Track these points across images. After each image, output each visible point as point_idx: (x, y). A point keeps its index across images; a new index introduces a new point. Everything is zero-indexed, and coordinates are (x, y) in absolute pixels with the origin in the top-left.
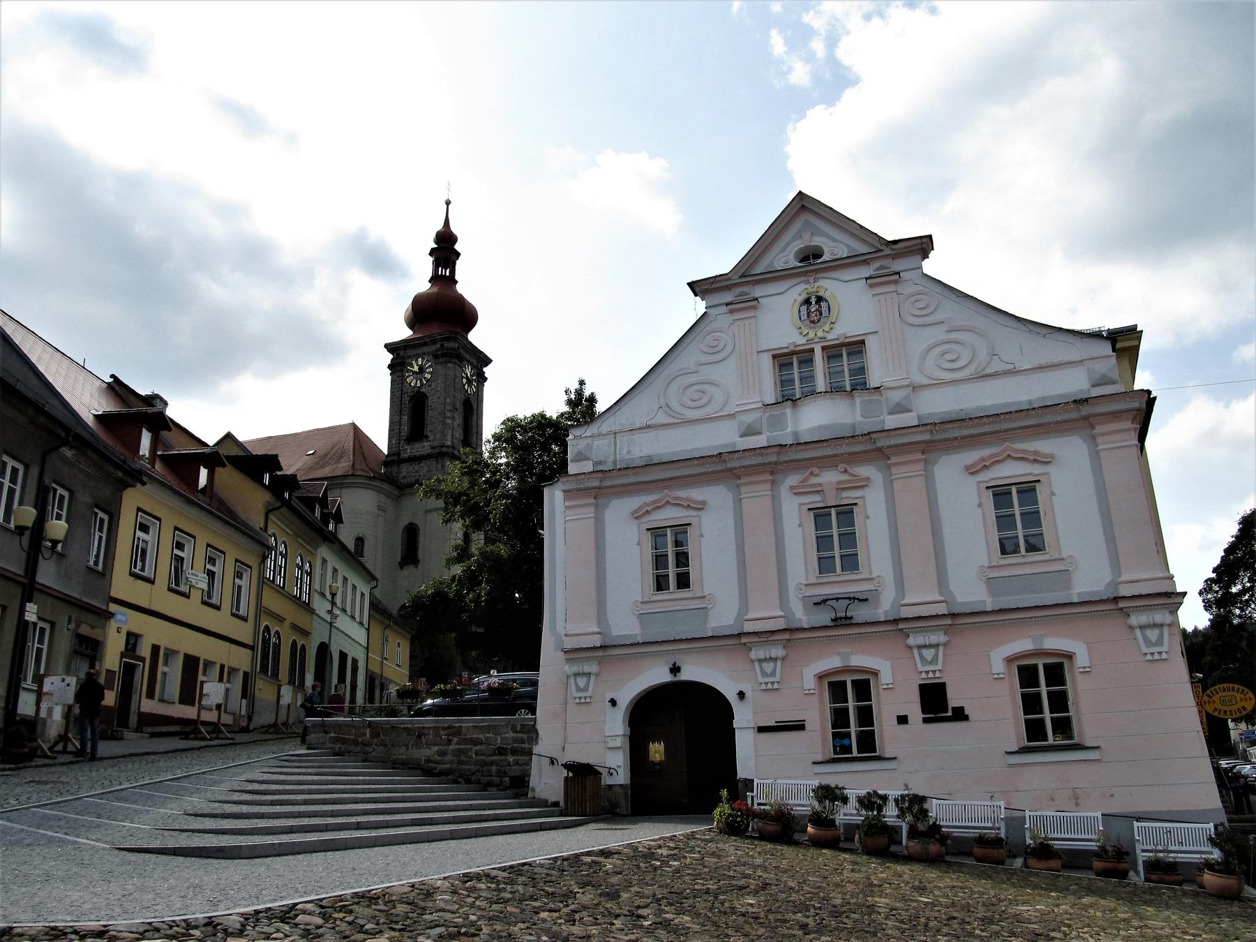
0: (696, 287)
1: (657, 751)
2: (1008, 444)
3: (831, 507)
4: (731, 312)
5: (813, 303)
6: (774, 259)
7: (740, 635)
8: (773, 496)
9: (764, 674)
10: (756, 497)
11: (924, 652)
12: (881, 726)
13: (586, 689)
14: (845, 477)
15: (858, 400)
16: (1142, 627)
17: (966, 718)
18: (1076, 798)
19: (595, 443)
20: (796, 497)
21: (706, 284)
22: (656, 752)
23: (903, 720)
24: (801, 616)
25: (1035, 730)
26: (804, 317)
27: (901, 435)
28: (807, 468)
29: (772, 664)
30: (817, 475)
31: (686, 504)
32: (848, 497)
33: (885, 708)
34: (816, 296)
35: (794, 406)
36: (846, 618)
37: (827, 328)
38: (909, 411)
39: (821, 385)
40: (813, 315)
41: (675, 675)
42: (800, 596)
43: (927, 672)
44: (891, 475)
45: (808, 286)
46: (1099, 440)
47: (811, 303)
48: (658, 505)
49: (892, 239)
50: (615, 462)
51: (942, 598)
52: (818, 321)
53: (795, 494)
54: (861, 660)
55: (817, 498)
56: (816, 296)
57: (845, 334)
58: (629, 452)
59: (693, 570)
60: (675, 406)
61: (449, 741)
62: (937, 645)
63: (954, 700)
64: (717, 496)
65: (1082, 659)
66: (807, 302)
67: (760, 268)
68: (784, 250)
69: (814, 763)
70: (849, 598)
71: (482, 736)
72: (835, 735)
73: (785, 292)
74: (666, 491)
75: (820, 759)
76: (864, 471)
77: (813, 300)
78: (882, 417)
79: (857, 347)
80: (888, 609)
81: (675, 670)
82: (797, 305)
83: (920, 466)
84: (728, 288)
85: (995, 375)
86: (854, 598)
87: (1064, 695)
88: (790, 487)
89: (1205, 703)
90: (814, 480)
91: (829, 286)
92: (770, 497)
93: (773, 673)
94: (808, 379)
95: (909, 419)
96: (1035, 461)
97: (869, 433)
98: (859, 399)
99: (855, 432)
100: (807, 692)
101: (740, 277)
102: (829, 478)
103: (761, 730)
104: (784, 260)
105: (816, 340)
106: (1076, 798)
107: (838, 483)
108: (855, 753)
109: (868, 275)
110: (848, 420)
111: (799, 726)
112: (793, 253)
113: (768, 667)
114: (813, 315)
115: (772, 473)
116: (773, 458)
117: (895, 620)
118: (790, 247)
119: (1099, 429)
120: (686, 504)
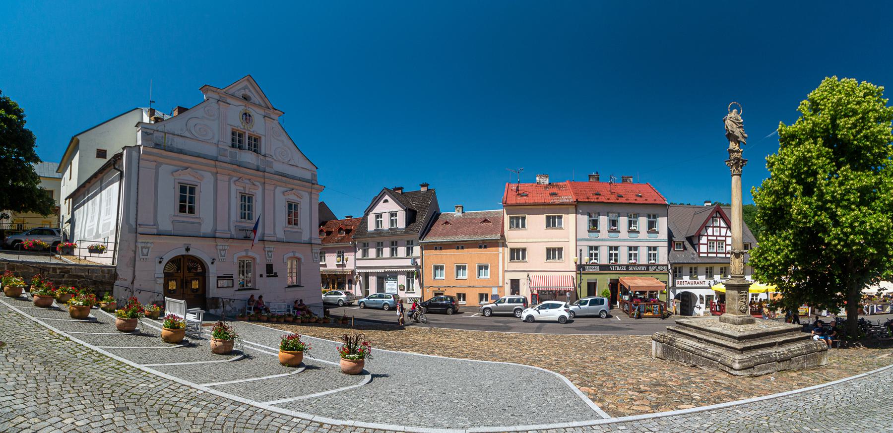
17: (277, 276)
23: (261, 276)
58: (171, 144)
61: (63, 276)
66: (245, 114)
71: (83, 274)
81: (188, 250)
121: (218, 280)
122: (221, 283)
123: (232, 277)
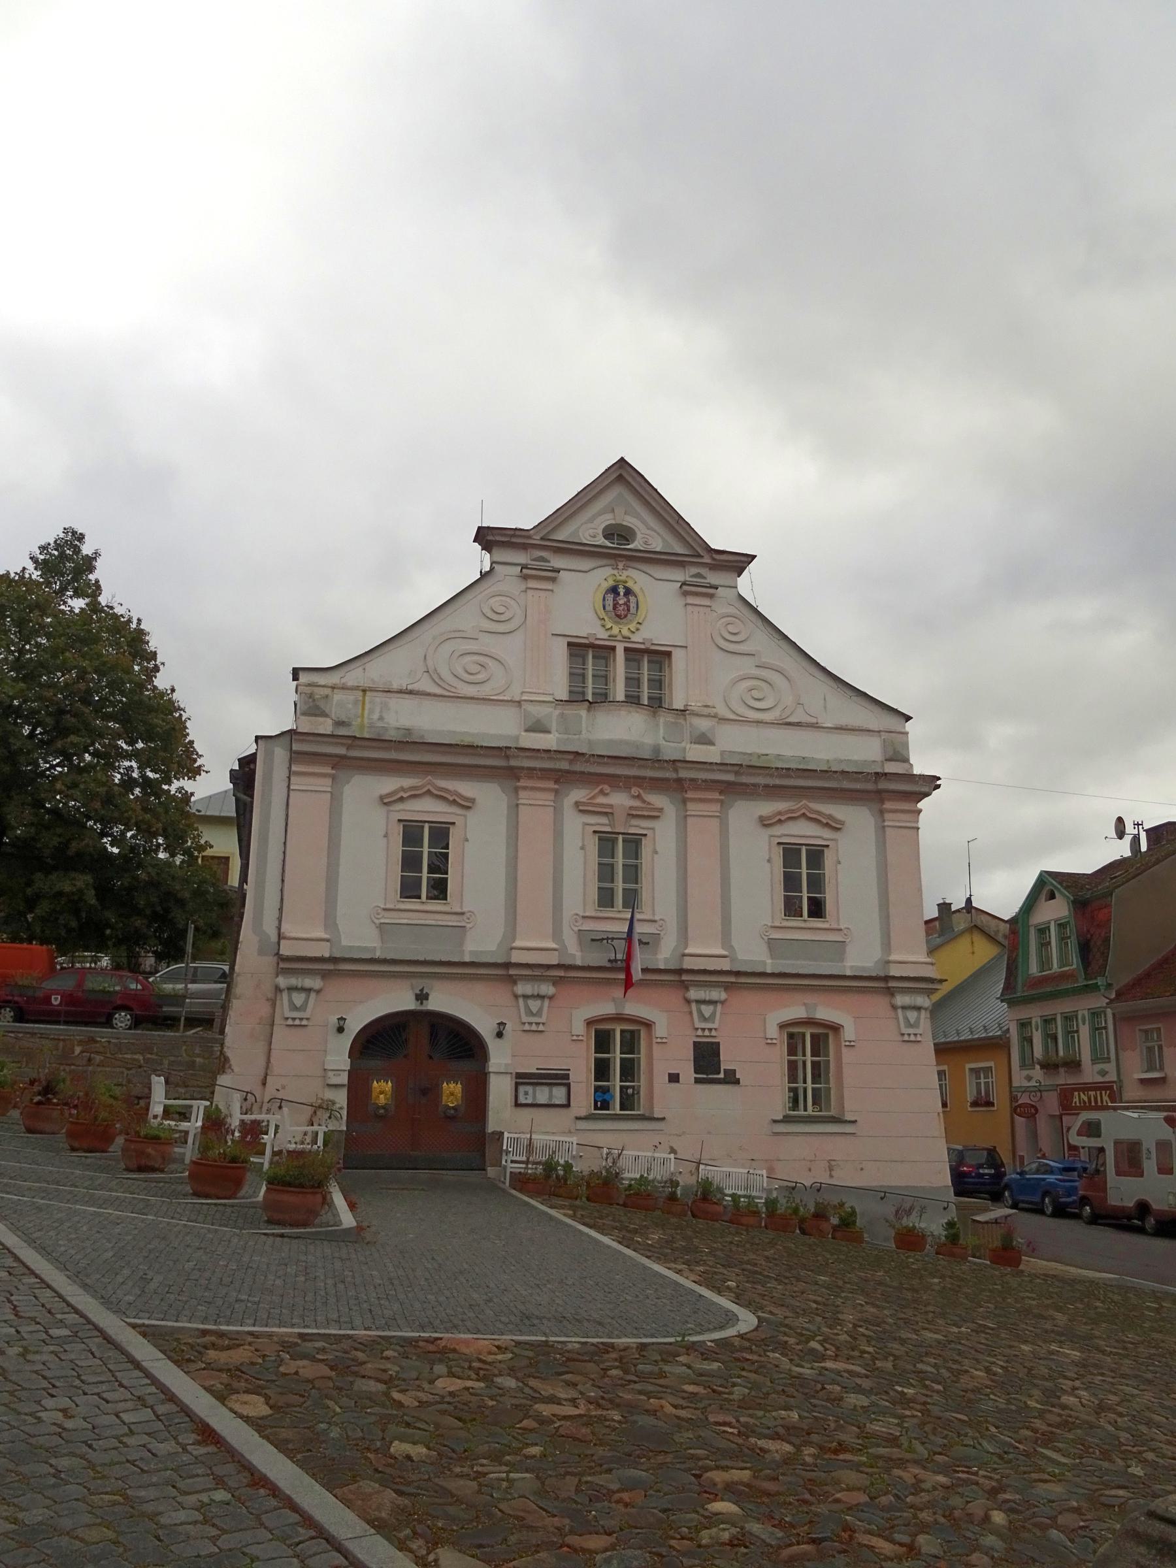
0: (486, 538)
1: (382, 1090)
3: (619, 833)
5: (622, 594)
6: (579, 528)
9: (530, 1013)
13: (303, 1008)
20: (581, 814)
22: (381, 1093)
24: (576, 954)
26: (610, 608)
29: (538, 1002)
30: (606, 795)
31: (451, 799)
32: (634, 829)
34: (625, 587)
37: (633, 627)
38: (712, 744)
40: (621, 608)
42: (576, 929)
45: (615, 572)
46: (887, 816)
47: (618, 594)
48: (416, 792)
50: (362, 727)
52: (626, 616)
56: (625, 587)
58: (381, 718)
60: (445, 673)
65: (849, 1033)
66: (614, 590)
67: (562, 535)
68: (591, 520)
74: (429, 777)
76: (657, 800)
77: (622, 591)
78: (683, 744)
80: (668, 956)
83: (715, 808)
84: (524, 547)
85: (798, 724)
91: (638, 579)
92: (552, 808)
93: (539, 1013)
96: (827, 825)
98: (664, 718)
100: (575, 1038)
105: (620, 638)
107: (631, 808)
110: (649, 740)
112: (603, 526)
113: (534, 1005)
114: (621, 608)
115: (557, 782)
119: (888, 805)
120: (451, 799)
121: (517, 1085)
122: (528, 1094)
123: (567, 1077)
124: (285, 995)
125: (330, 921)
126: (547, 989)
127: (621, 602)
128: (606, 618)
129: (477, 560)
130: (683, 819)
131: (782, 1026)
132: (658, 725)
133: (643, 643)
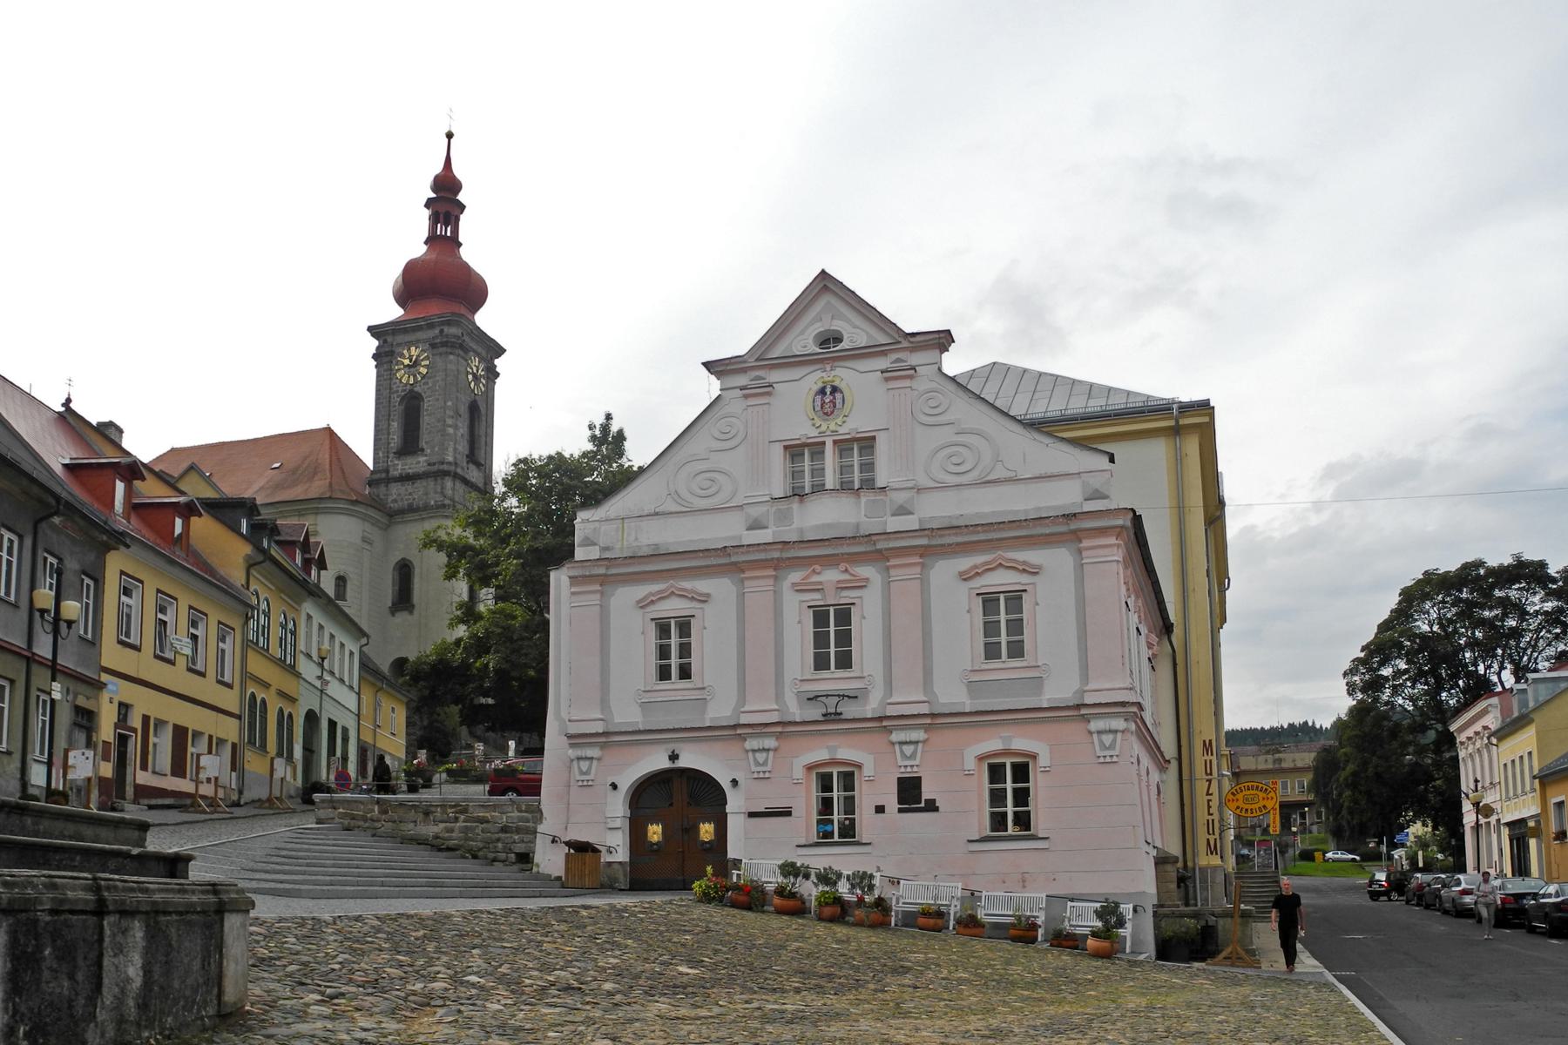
2: (1000, 552)
3: (829, 606)
4: (746, 397)
5: (828, 393)
6: (792, 342)
7: (735, 727)
8: (775, 591)
9: (757, 764)
10: (759, 587)
11: (905, 748)
12: (861, 815)
14: (847, 577)
15: (863, 500)
16: (1099, 732)
17: (936, 809)
18: (1024, 881)
19: (603, 528)
21: (723, 365)
23: (880, 809)
24: (795, 711)
25: (998, 821)
26: (818, 408)
27: (903, 538)
28: (811, 565)
29: (764, 755)
30: (819, 573)
32: (846, 597)
33: (865, 799)
35: (801, 501)
36: (837, 714)
38: (912, 513)
39: (830, 480)
41: (674, 762)
42: (796, 691)
43: (906, 767)
44: (889, 577)
49: (911, 332)
51: (925, 699)
52: (832, 412)
53: (797, 591)
54: (846, 753)
55: (817, 596)
57: (857, 429)
59: (694, 661)
62: (917, 742)
63: (926, 794)
64: (720, 588)
65: (1044, 760)
66: (822, 392)
67: (777, 352)
69: (797, 846)
70: (839, 696)
72: (819, 822)
73: (800, 379)
75: (803, 842)
76: (865, 571)
77: (828, 390)
78: (885, 518)
79: (867, 444)
81: (674, 757)
82: (812, 393)
83: (918, 569)
84: (744, 371)
86: (844, 696)
87: (1026, 791)
88: (793, 584)
89: (1229, 801)
90: (815, 578)
93: (765, 763)
94: (818, 472)
95: (909, 523)
97: (870, 535)
98: (865, 497)
99: (857, 532)
100: (795, 781)
101: (756, 360)
102: (831, 576)
103: (752, 815)
104: (802, 343)
106: (1024, 881)
107: (839, 582)
108: (836, 838)
109: (884, 367)
111: (786, 813)
113: (761, 757)
116: (776, 555)
117: (880, 717)
118: (809, 331)
124: (575, 763)
125: (604, 703)
126: (770, 743)
127: (827, 401)
128: (815, 418)
129: (711, 387)
130: (887, 585)
131: (981, 758)
132: (860, 502)
133: (849, 434)
